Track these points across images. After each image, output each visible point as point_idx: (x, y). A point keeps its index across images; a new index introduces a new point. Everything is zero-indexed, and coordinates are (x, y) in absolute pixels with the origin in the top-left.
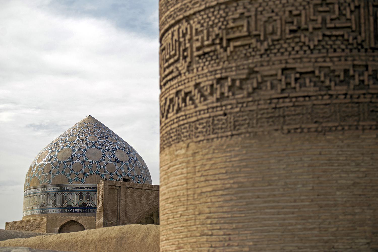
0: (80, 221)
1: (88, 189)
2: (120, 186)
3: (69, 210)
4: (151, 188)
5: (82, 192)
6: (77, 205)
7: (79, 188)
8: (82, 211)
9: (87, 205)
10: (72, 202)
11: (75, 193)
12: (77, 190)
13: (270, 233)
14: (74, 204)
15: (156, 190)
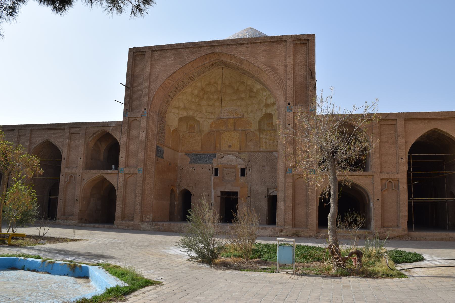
4: (182, 46)
15: (188, 48)
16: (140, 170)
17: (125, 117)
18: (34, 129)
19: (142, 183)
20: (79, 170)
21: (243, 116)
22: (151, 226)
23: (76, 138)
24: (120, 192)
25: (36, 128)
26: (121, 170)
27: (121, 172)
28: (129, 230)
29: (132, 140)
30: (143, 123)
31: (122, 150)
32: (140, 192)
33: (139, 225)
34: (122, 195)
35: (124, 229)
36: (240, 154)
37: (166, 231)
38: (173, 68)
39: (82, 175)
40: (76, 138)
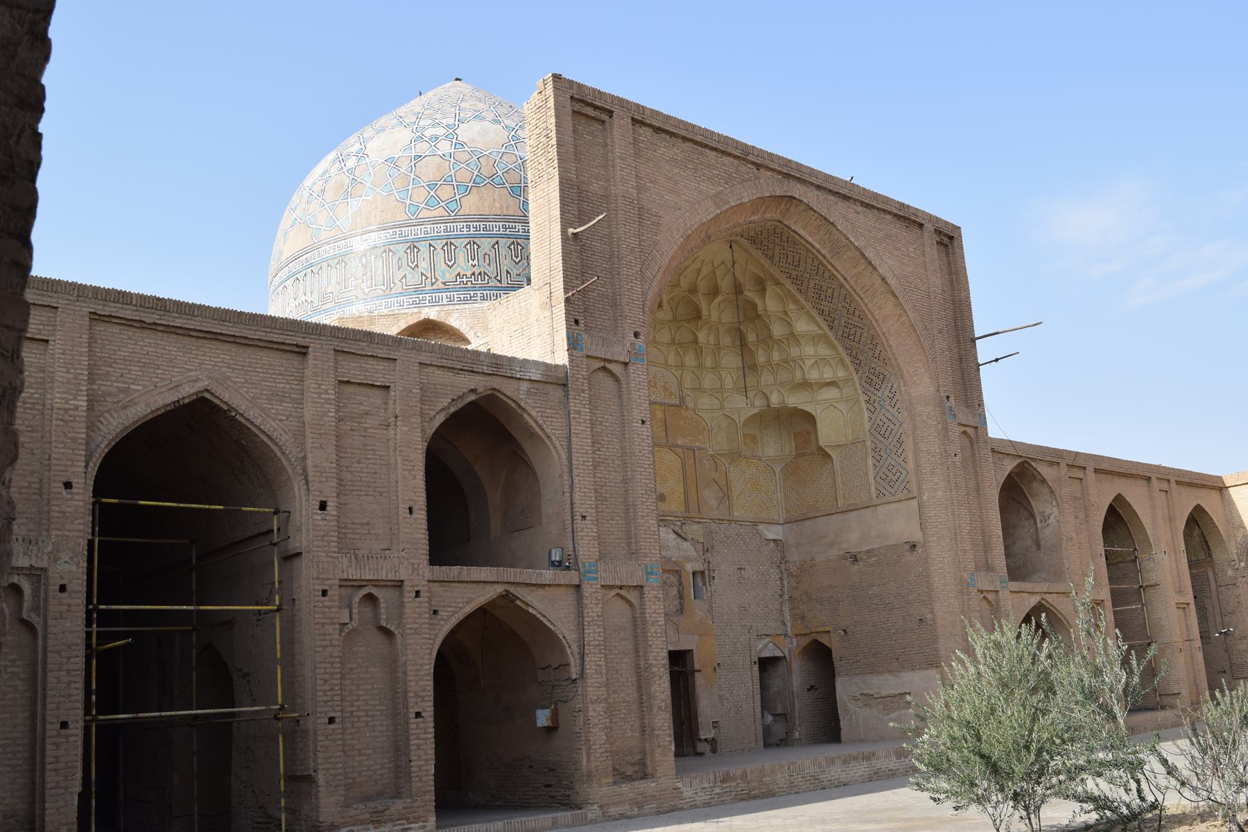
0: (452, 320)
1: (472, 229)
2: (613, 109)
3: (411, 300)
5: (452, 241)
6: (439, 282)
7: (442, 230)
8: (456, 299)
9: (473, 279)
10: (422, 274)
11: (430, 245)
12: (436, 234)
13: (839, 479)
14: (429, 279)
15: (730, 155)
16: (650, 573)
17: (575, 353)
18: (108, 319)
19: (663, 622)
20: (414, 570)
21: (682, 399)
22: (712, 785)
23: (362, 408)
24: (596, 665)
25: (128, 313)
26: (590, 572)
27: (590, 579)
28: (647, 815)
29: (599, 450)
30: (639, 389)
31: (580, 488)
32: (663, 659)
33: (675, 789)
34: (604, 676)
35: (626, 818)
37: (755, 797)
38: (696, 206)
39: (429, 591)
40: (362, 408)
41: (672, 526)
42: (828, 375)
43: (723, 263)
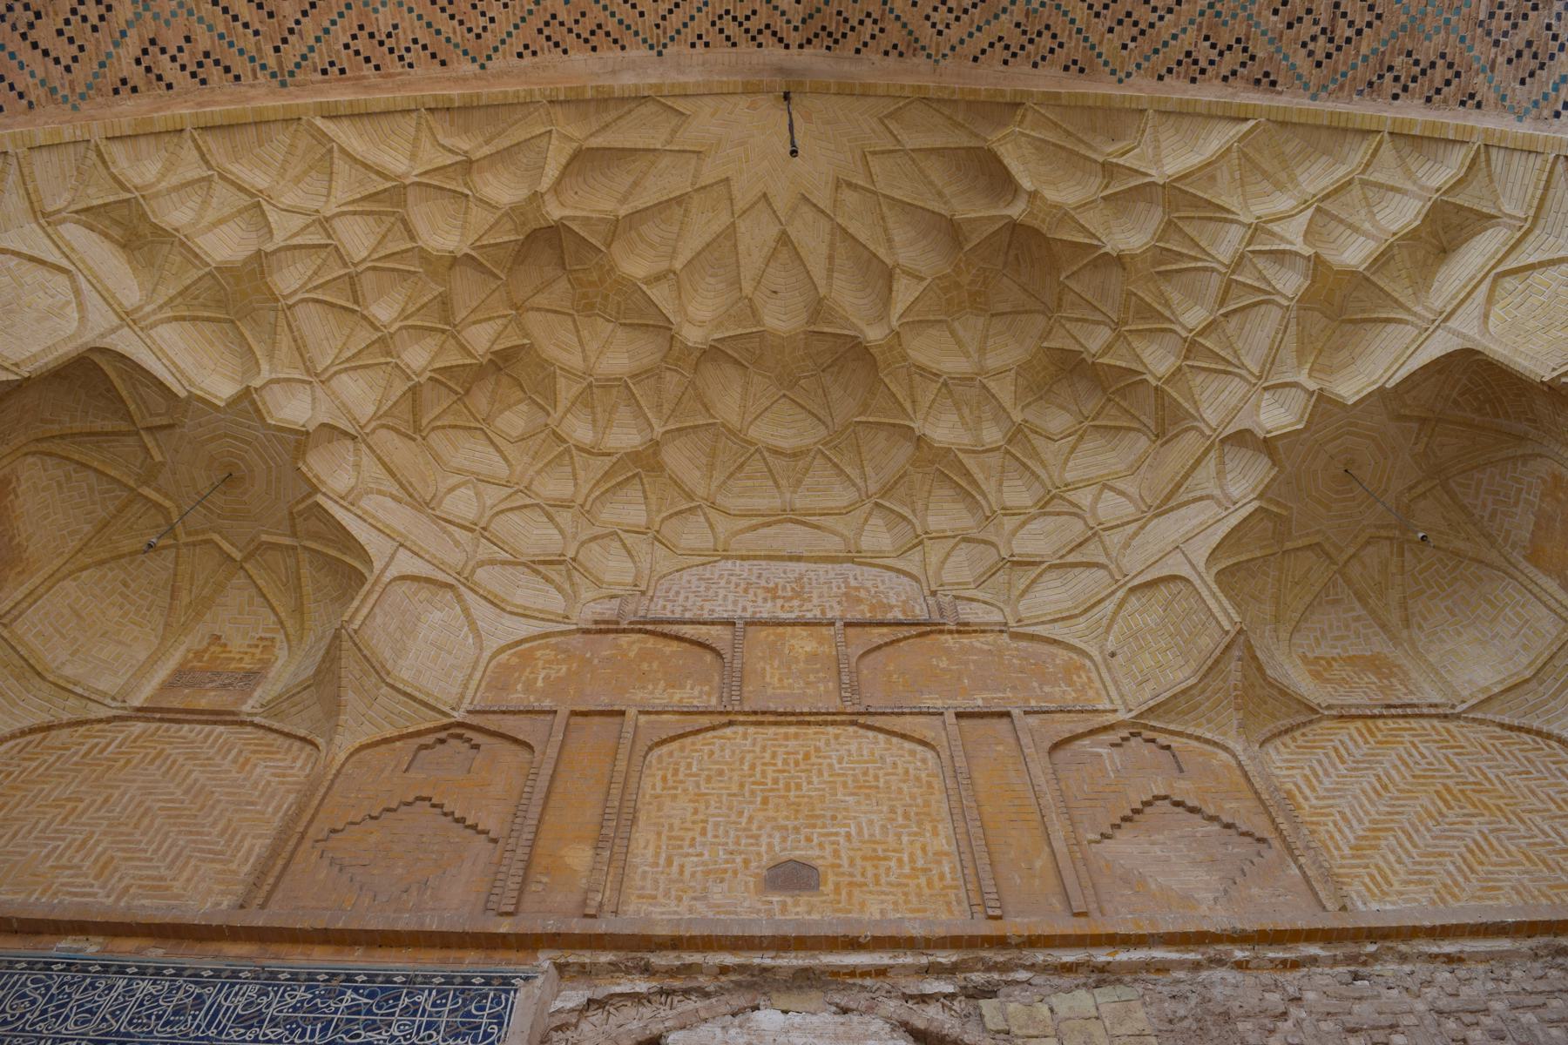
36: (986, 1005)
41: (892, 1006)
42: (1402, 214)
43: (838, 184)
